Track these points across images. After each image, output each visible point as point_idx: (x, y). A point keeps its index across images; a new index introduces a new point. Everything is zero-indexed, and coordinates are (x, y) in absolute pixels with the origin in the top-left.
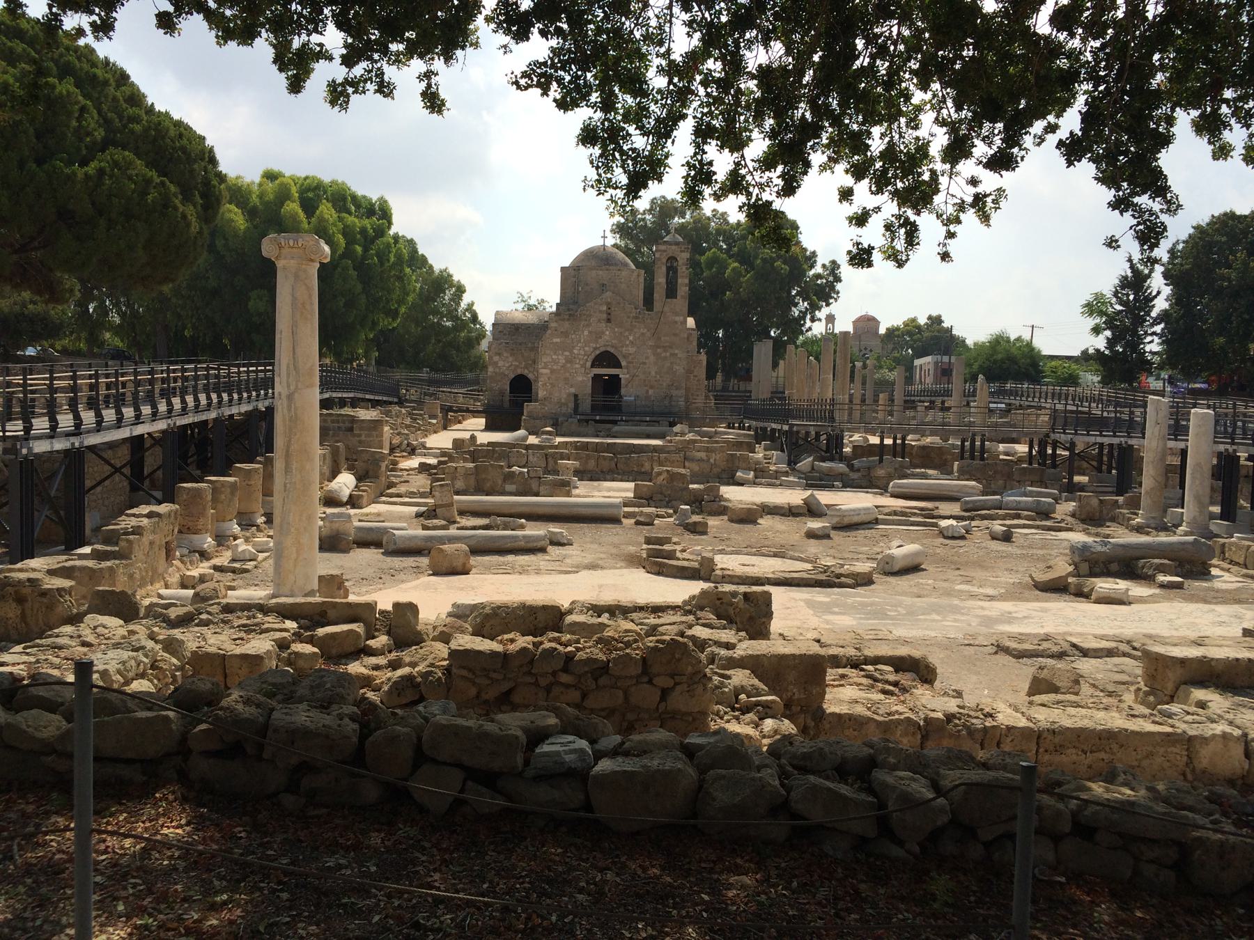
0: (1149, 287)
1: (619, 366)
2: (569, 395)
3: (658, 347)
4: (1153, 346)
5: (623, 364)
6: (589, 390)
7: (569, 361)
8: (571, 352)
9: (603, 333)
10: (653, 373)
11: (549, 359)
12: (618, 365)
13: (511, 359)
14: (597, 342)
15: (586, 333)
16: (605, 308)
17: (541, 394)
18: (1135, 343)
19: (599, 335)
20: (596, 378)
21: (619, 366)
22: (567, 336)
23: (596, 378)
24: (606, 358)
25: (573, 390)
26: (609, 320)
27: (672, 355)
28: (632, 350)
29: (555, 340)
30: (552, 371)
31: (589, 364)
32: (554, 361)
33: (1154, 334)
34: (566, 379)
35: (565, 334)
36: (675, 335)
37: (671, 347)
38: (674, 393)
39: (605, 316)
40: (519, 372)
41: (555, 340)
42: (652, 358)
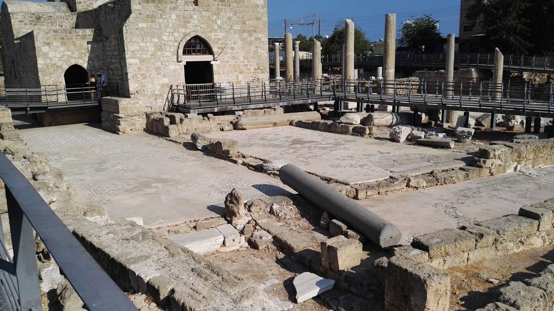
1: (211, 52)
2: (163, 86)
3: (244, 31)
5: (215, 50)
7: (160, 47)
8: (160, 38)
9: (191, 17)
10: (241, 59)
11: (136, 47)
12: (208, 50)
13: (62, 49)
14: (185, 27)
15: (174, 16)
17: (133, 86)
20: (189, 67)
21: (211, 52)
22: (153, 22)
24: (198, 44)
25: (166, 80)
27: (256, 39)
28: (220, 35)
29: (141, 25)
30: (142, 61)
31: (181, 51)
32: (142, 49)
34: (158, 69)
35: (151, 18)
36: (258, 19)
37: (255, 31)
40: (73, 62)
41: (141, 25)
42: (240, 43)
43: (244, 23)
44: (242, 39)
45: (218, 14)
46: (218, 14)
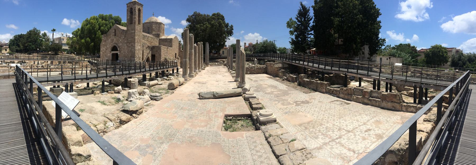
0: (309, 16)
1: (117, 50)
3: (127, 43)
4: (311, 37)
6: (111, 58)
7: (106, 50)
16: (114, 31)
18: (305, 38)
19: (113, 40)
20: (113, 54)
23: (113, 54)
24: (114, 48)
26: (115, 35)
28: (121, 44)
33: (311, 34)
35: (105, 41)
36: (132, 38)
38: (132, 59)
39: (114, 34)
42: (126, 47)
43: (128, 40)
44: (127, 46)
45: (120, 38)
46: (120, 38)
